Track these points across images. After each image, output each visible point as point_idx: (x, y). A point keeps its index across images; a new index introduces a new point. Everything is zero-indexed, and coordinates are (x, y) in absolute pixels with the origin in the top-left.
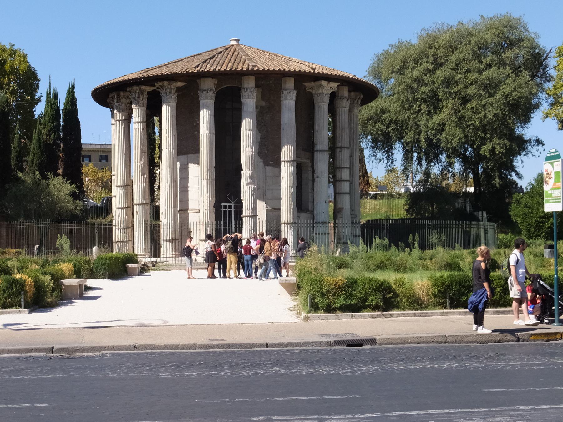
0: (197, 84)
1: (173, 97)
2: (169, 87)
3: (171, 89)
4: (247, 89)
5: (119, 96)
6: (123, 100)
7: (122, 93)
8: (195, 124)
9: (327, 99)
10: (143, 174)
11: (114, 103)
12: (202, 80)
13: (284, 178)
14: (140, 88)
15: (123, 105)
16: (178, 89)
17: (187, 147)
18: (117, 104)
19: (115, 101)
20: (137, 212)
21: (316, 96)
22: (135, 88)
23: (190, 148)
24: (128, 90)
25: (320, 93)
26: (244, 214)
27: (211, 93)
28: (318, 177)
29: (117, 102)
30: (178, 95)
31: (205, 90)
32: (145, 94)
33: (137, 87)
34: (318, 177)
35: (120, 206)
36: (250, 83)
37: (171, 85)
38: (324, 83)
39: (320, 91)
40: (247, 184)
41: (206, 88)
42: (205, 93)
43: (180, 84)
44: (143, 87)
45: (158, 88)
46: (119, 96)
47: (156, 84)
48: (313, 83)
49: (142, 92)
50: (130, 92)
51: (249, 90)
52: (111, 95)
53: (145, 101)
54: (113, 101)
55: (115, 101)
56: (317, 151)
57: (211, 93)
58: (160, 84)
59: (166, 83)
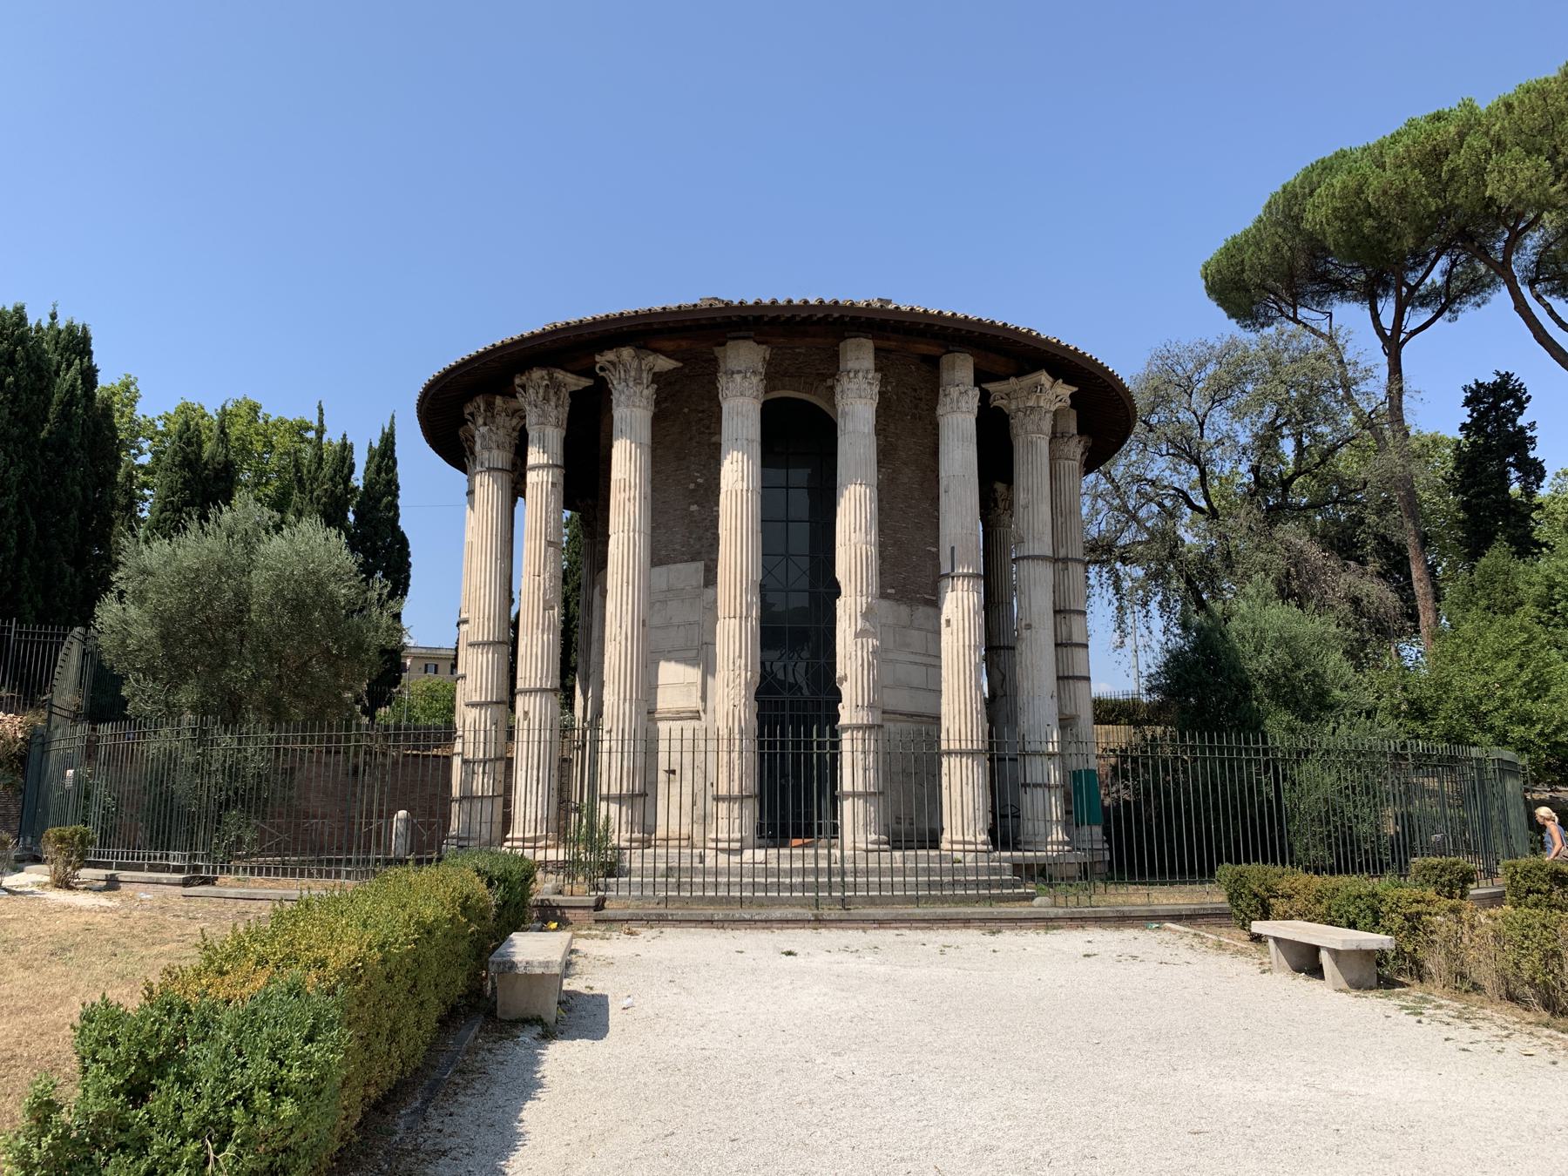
0: (716, 359)
1: (646, 392)
2: (635, 364)
3: (639, 370)
4: (856, 372)
5: (490, 406)
6: (500, 420)
7: (499, 401)
8: (692, 486)
9: (1047, 425)
10: (548, 607)
12: (730, 344)
13: (953, 622)
14: (551, 378)
15: (501, 432)
16: (657, 378)
17: (683, 529)
18: (484, 429)
19: (480, 421)
20: (526, 713)
21: (1021, 414)
22: (537, 374)
23: (677, 547)
24: (517, 381)
25: (1032, 408)
26: (844, 719)
27: (755, 380)
28: (1029, 627)
29: (485, 424)
30: (657, 392)
31: (739, 372)
32: (564, 393)
33: (544, 373)
34: (1029, 627)
35: (476, 699)
36: (859, 358)
37: (640, 360)
38: (1044, 378)
39: (1031, 404)
40: (856, 636)
41: (742, 368)
42: (738, 378)
43: (664, 364)
44: (560, 375)
45: (602, 369)
46: (490, 406)
47: (598, 358)
48: (1013, 380)
49: (556, 386)
50: (523, 387)
52: (469, 409)
53: (564, 412)
54: (474, 423)
55: (480, 421)
56: (1028, 558)
57: (755, 380)
58: (610, 356)
59: (627, 353)
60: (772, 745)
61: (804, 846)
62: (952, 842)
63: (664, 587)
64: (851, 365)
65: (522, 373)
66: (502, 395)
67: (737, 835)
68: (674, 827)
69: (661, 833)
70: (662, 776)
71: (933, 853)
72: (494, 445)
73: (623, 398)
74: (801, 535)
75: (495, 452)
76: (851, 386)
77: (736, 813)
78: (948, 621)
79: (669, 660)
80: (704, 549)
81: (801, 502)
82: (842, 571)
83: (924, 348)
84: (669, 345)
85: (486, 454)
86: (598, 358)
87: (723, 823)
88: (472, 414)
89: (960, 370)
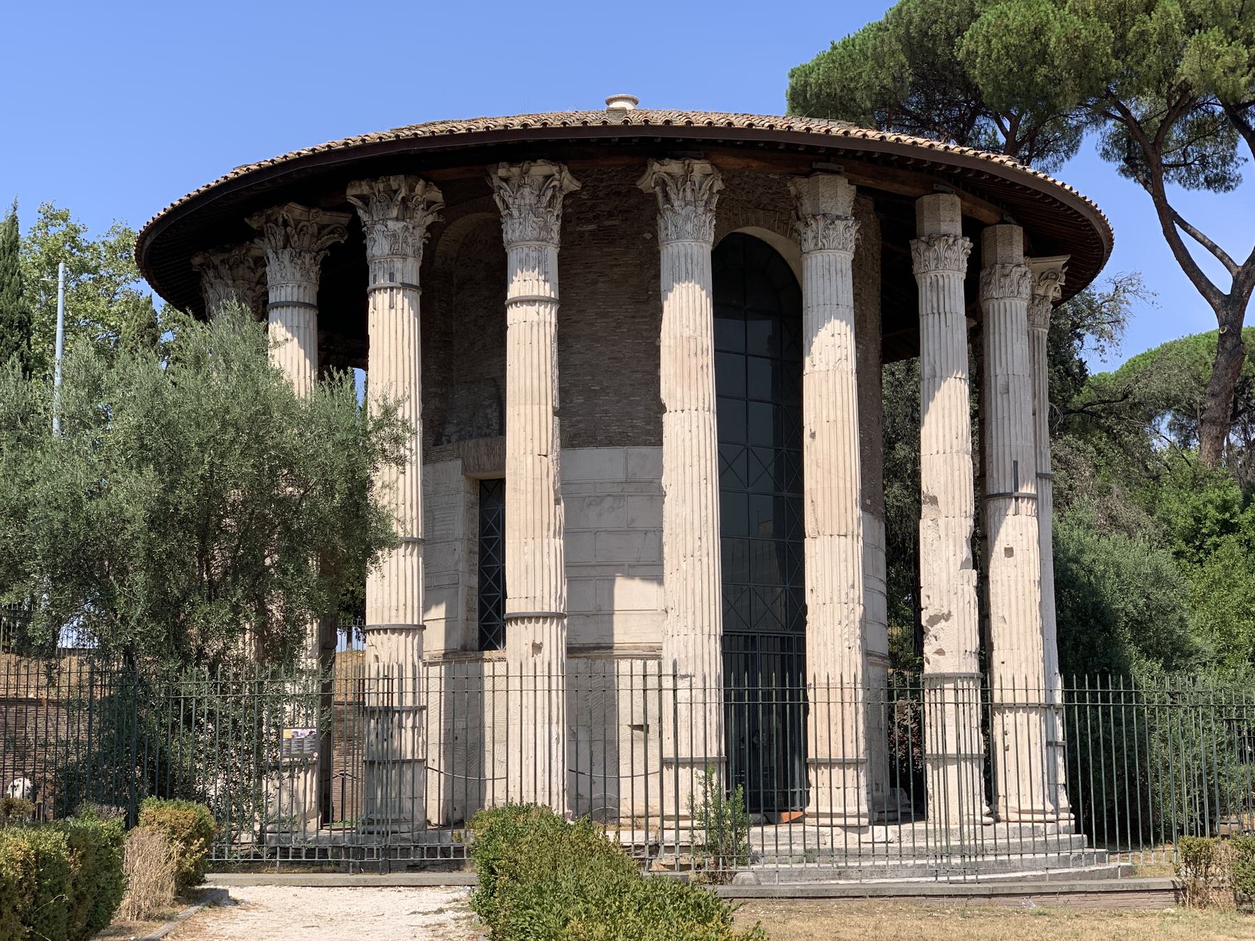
5: (412, 189)
6: (419, 214)
11: (384, 221)
12: (823, 178)
15: (420, 232)
22: (540, 169)
23: (639, 423)
24: (502, 172)
29: (397, 219)
31: (838, 217)
33: (555, 169)
39: (1041, 292)
42: (840, 225)
50: (506, 180)
51: (960, 241)
58: (675, 167)
59: (700, 167)
60: (740, 696)
61: (791, 822)
62: (1020, 812)
63: (621, 477)
64: (945, 227)
65: (513, 162)
66: (427, 180)
67: (852, 809)
68: (654, 802)
69: (625, 809)
70: (625, 732)
71: (920, 826)
72: (410, 251)
73: (689, 227)
74: (763, 414)
75: (410, 260)
76: (949, 254)
77: (851, 783)
78: (1009, 552)
79: (631, 576)
80: (646, 427)
81: (763, 371)
82: (930, 481)
83: (985, 213)
84: (732, 162)
85: (398, 264)
86: (656, 167)
87: (838, 794)
88: (364, 199)
89: (1011, 244)
